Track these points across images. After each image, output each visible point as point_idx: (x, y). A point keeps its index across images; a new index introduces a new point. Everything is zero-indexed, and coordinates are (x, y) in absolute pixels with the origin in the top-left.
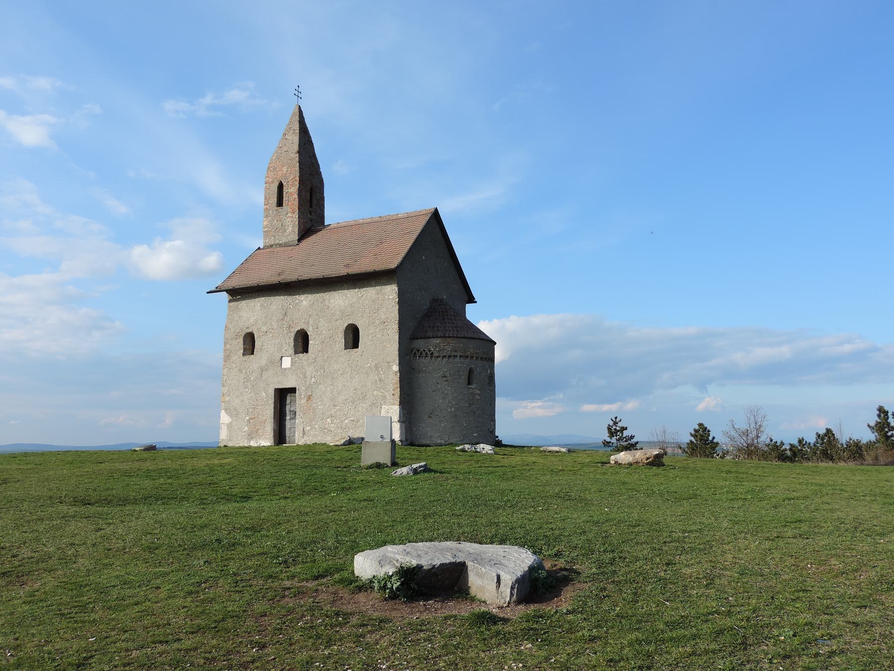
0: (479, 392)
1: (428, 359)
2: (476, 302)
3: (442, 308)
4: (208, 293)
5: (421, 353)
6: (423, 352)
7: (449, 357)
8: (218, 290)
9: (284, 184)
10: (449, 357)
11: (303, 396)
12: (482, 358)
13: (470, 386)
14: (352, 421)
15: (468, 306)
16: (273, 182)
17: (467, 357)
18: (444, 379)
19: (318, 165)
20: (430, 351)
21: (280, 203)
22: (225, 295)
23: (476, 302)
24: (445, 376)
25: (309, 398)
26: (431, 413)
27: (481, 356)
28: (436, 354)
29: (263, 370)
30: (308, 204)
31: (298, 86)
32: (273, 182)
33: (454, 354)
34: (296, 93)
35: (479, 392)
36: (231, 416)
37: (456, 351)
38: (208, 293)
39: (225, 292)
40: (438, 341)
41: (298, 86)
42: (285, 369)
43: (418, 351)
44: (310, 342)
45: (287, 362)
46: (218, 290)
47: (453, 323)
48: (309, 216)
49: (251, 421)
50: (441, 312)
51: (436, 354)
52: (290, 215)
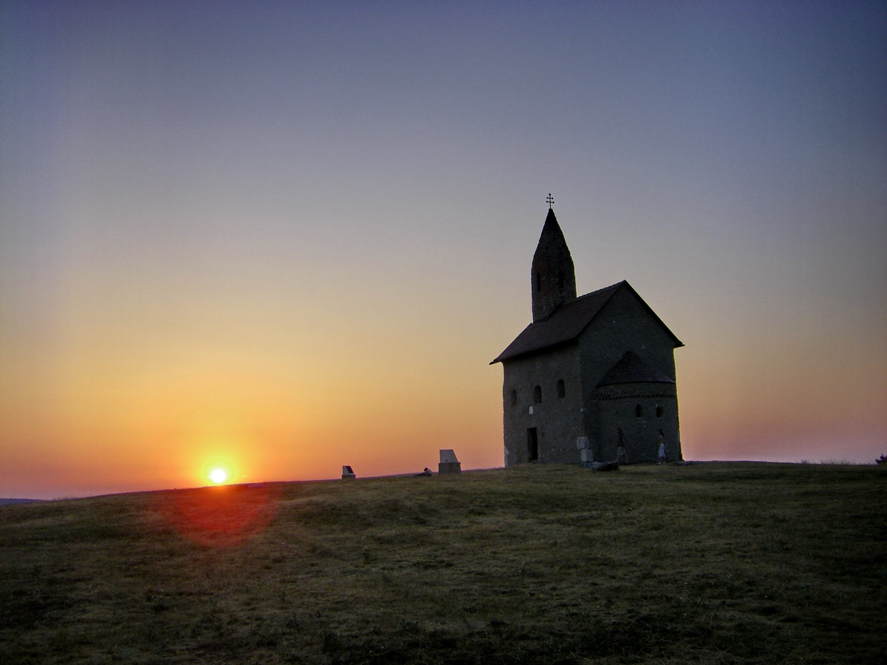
0: (646, 422)
1: (608, 400)
2: (684, 345)
4: (490, 364)
5: (604, 397)
7: (621, 398)
8: (496, 361)
10: (621, 398)
13: (637, 418)
15: (676, 350)
19: (569, 253)
20: (608, 394)
21: (539, 290)
22: (500, 365)
23: (684, 345)
28: (612, 397)
31: (550, 195)
33: (624, 395)
34: (548, 200)
35: (646, 422)
37: (625, 393)
38: (491, 363)
39: (501, 362)
40: (612, 387)
43: (602, 395)
45: (531, 411)
46: (496, 361)
48: (559, 294)
51: (612, 397)
52: (544, 297)
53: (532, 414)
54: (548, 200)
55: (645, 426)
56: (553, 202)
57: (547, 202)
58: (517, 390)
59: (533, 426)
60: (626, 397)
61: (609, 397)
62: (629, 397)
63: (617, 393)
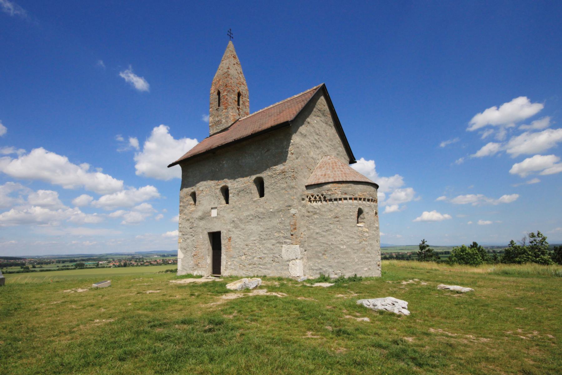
3: (332, 161)
5: (315, 198)
6: (317, 196)
9: (221, 91)
10: (340, 199)
11: (225, 238)
12: (368, 200)
13: (358, 225)
14: (260, 258)
16: (214, 92)
17: (356, 199)
18: (337, 219)
20: (322, 195)
22: (178, 167)
24: (336, 217)
25: (230, 239)
26: (325, 251)
27: (368, 198)
28: (328, 198)
29: (201, 218)
30: (236, 103)
31: (230, 30)
32: (214, 92)
34: (229, 34)
36: (183, 253)
41: (230, 30)
42: (214, 218)
44: (230, 195)
47: (342, 171)
49: (195, 256)
50: (331, 164)
51: (328, 198)
53: (216, 217)
54: (229, 34)
55: (367, 235)
56: (233, 38)
57: (228, 34)
58: (197, 193)
59: (216, 230)
60: (346, 199)
61: (325, 198)
62: (350, 199)
63: (336, 193)
